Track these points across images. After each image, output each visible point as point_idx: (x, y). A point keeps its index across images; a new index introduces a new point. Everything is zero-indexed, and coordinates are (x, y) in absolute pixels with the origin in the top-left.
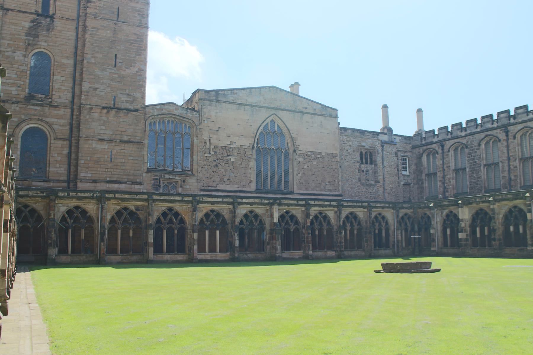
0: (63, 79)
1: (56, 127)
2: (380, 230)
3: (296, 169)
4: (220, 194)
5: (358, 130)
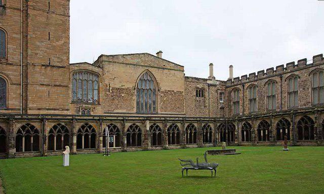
2: (207, 133)
3: (159, 100)
4: (116, 115)
5: (196, 78)
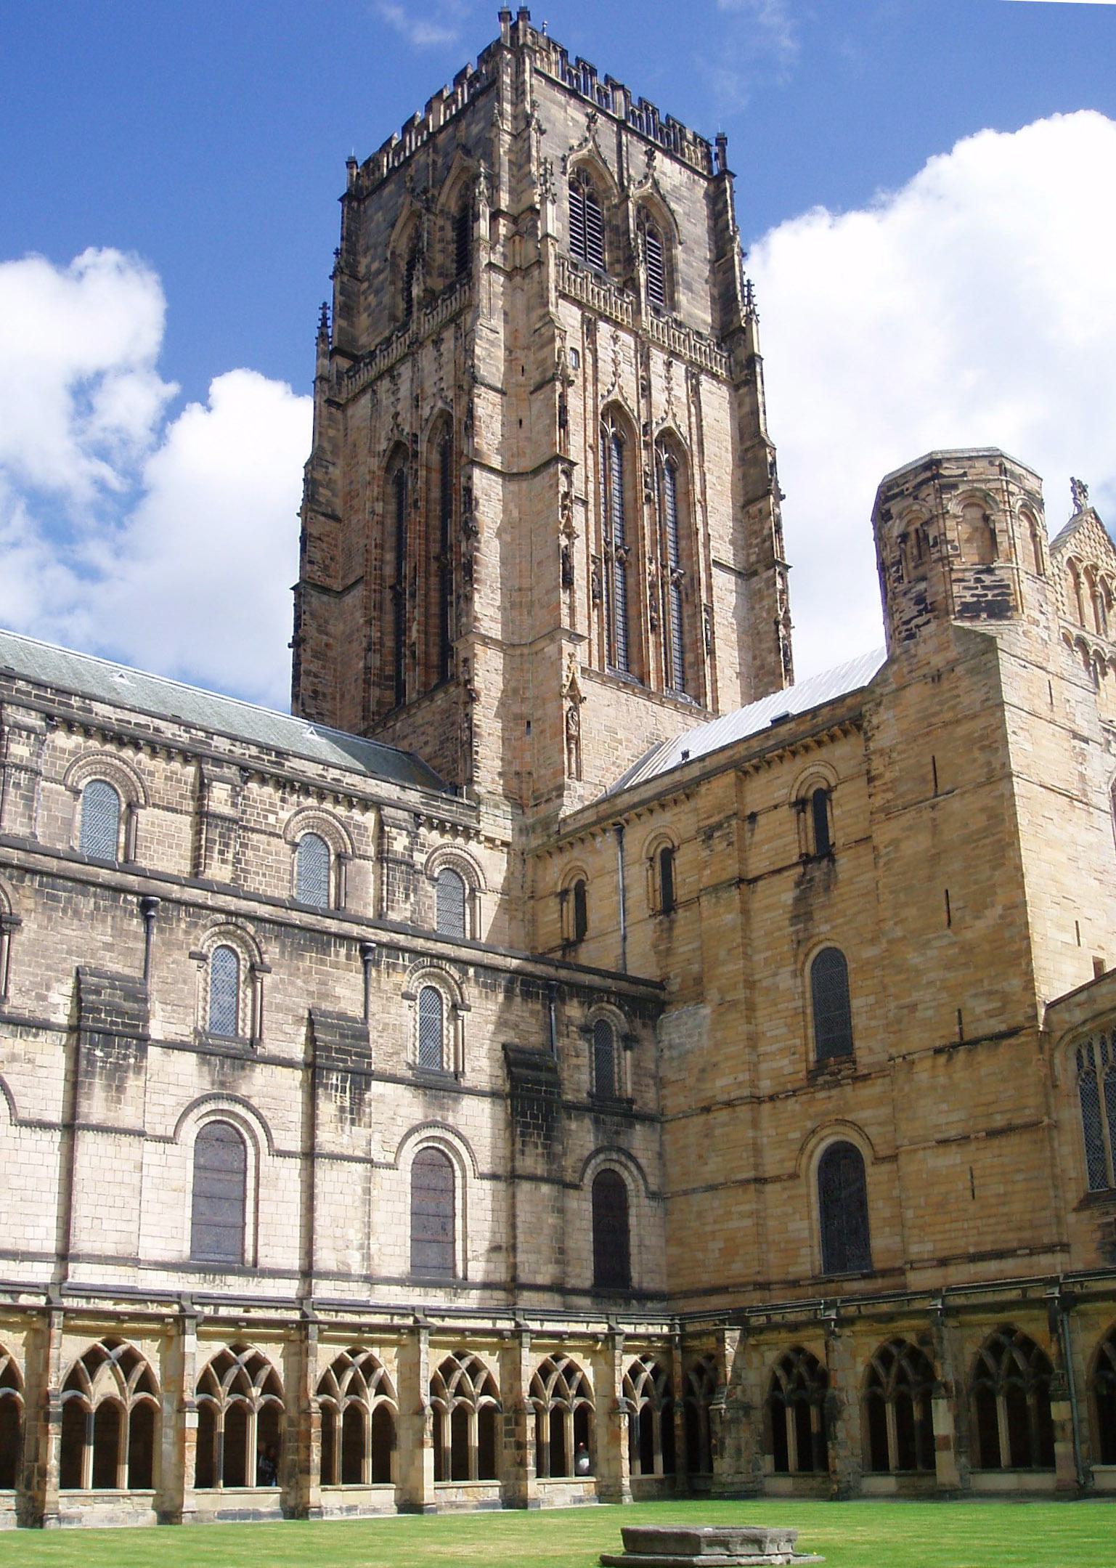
0: (871, 1000)
1: (872, 1131)
